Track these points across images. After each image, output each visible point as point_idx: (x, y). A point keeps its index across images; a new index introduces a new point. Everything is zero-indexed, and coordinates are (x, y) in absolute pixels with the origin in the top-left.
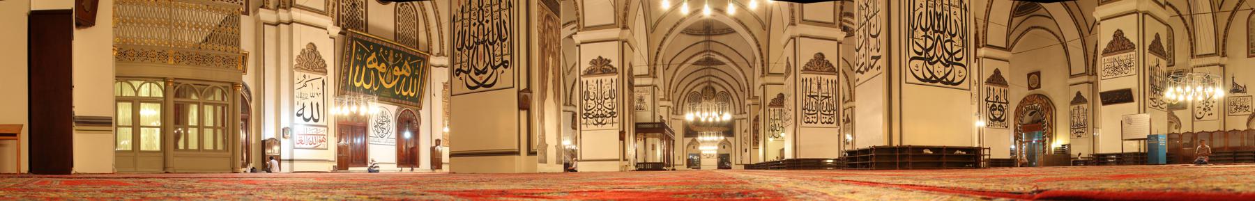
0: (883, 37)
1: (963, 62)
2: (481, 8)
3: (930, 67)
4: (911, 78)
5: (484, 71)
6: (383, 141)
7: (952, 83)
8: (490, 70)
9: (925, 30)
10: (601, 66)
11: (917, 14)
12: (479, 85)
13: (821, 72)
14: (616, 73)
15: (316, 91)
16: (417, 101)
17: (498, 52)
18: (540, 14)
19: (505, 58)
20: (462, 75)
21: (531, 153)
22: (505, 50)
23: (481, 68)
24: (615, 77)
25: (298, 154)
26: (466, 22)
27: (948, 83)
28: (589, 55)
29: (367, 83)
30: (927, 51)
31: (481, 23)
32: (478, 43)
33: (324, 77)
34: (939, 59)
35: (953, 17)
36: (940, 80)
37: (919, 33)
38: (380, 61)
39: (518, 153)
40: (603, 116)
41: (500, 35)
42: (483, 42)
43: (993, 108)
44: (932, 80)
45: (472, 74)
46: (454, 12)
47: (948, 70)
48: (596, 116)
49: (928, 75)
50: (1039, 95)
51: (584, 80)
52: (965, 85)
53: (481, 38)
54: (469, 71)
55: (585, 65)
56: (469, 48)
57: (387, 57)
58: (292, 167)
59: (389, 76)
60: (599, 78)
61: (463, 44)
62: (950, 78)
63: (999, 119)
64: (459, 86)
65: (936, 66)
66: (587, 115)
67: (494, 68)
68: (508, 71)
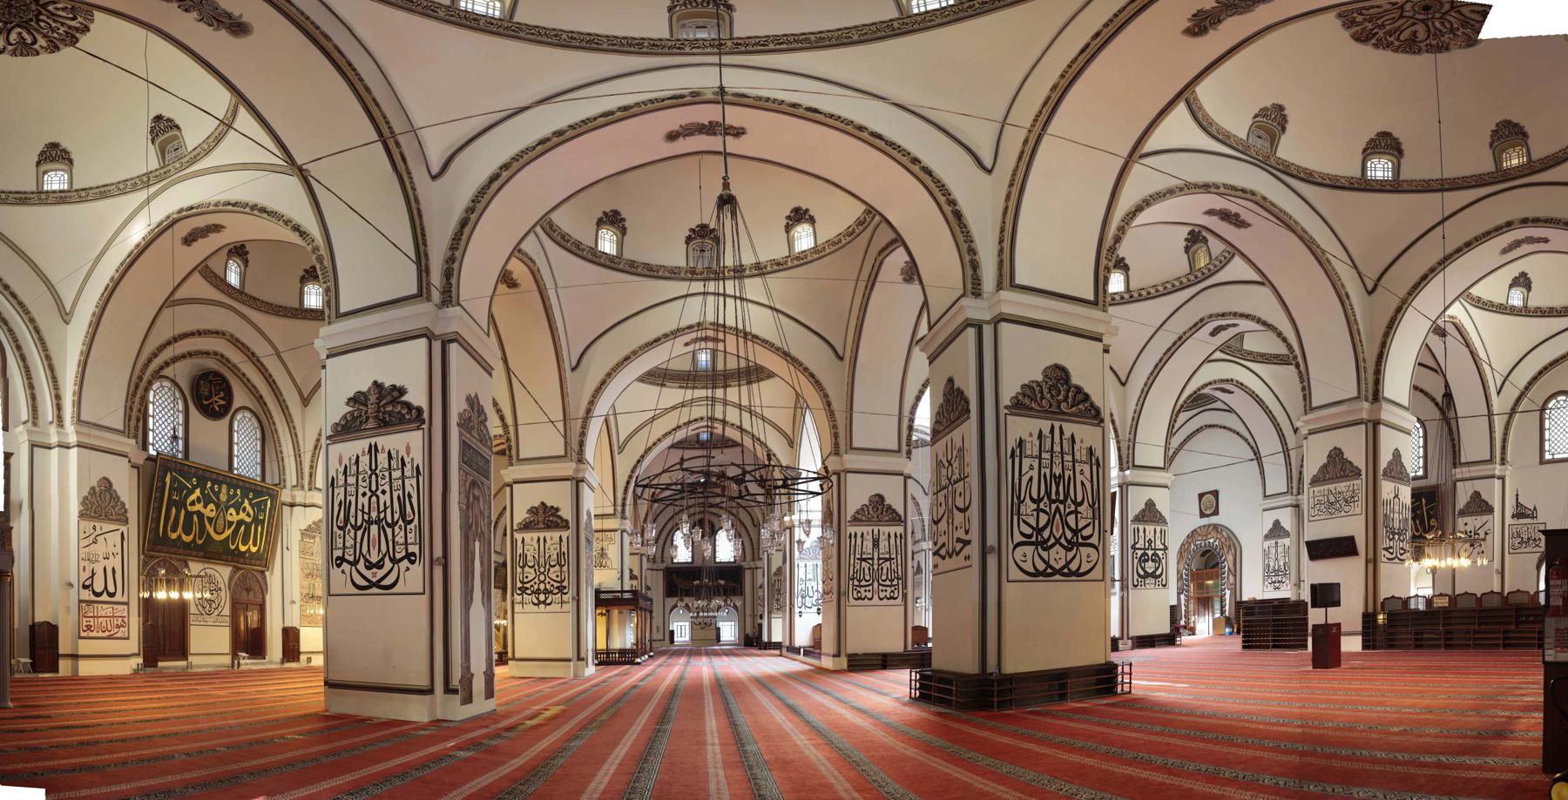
1: (1094, 540)
2: (374, 472)
3: (1044, 554)
4: (1015, 573)
5: (379, 565)
7: (1077, 573)
8: (388, 564)
9: (1037, 501)
10: (545, 518)
11: (1025, 480)
12: (372, 585)
13: (879, 522)
14: (567, 527)
17: (400, 539)
18: (462, 482)
19: (412, 549)
20: (345, 566)
21: (449, 690)
23: (374, 559)
24: (565, 534)
25: (85, 647)
26: (351, 489)
27: (1071, 574)
28: (525, 500)
30: (1040, 531)
31: (374, 493)
32: (370, 522)
34: (1058, 541)
35: (1079, 478)
40: (546, 592)
42: (378, 521)
45: (361, 566)
46: (332, 473)
47: (1070, 555)
48: (538, 592)
49: (1041, 566)
53: (374, 515)
54: (355, 563)
55: (521, 515)
60: (542, 535)
61: (347, 520)
64: (340, 579)
65: (1053, 551)
66: (523, 590)
67: (394, 561)
68: (417, 571)
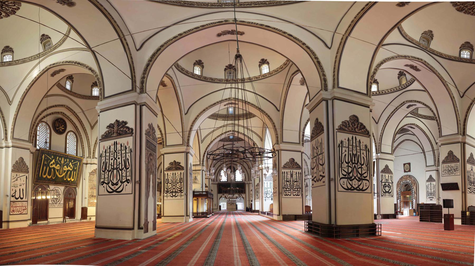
0: (326, 166)
1: (368, 178)
2: (115, 151)
3: (351, 182)
4: (340, 189)
5: (116, 184)
6: (56, 206)
8: (120, 184)
10: (176, 166)
12: (114, 191)
13: (293, 168)
15: (22, 182)
16: (76, 184)
17: (124, 175)
18: (146, 154)
20: (105, 185)
21: (140, 228)
22: (128, 174)
23: (115, 182)
24: (182, 172)
26: (107, 158)
27: (360, 190)
28: (168, 160)
29: (49, 175)
31: (115, 159)
32: (114, 169)
33: (27, 175)
34: (355, 178)
36: (356, 189)
37: (345, 165)
38: (56, 163)
39: (133, 229)
40: (176, 192)
41: (125, 166)
42: (117, 169)
43: (385, 186)
44: (351, 189)
45: (110, 185)
46: (101, 152)
49: (350, 187)
50: (410, 176)
51: (166, 173)
52: (369, 190)
53: (115, 166)
54: (108, 183)
55: (167, 165)
56: (109, 171)
57: (60, 161)
58: (8, 226)
59: (61, 171)
60: (174, 172)
61: (106, 168)
62: (361, 187)
63: (388, 192)
64: (103, 189)
65: (354, 181)
66: (167, 192)
68: (130, 185)
